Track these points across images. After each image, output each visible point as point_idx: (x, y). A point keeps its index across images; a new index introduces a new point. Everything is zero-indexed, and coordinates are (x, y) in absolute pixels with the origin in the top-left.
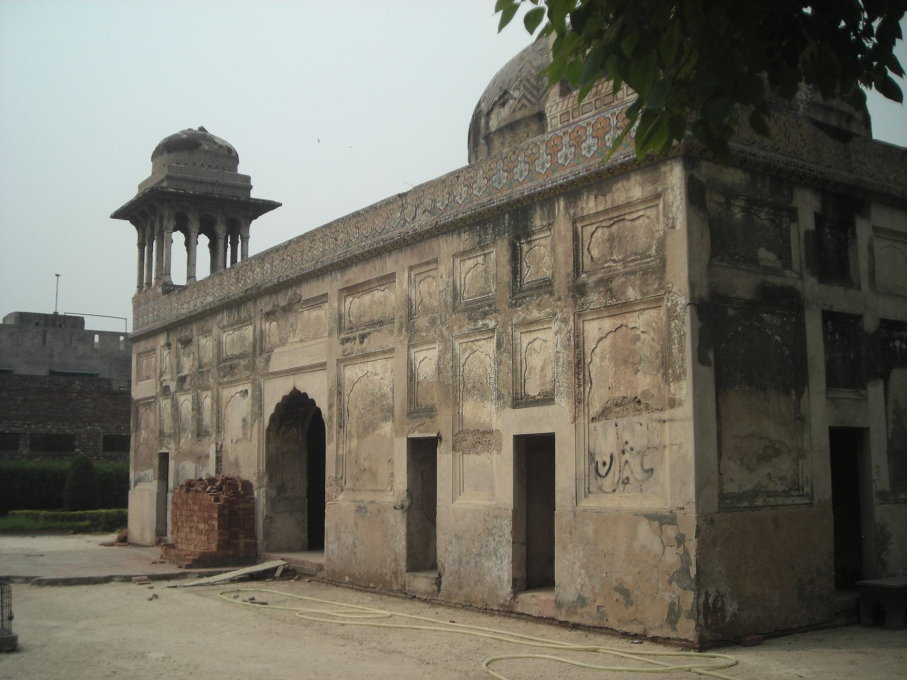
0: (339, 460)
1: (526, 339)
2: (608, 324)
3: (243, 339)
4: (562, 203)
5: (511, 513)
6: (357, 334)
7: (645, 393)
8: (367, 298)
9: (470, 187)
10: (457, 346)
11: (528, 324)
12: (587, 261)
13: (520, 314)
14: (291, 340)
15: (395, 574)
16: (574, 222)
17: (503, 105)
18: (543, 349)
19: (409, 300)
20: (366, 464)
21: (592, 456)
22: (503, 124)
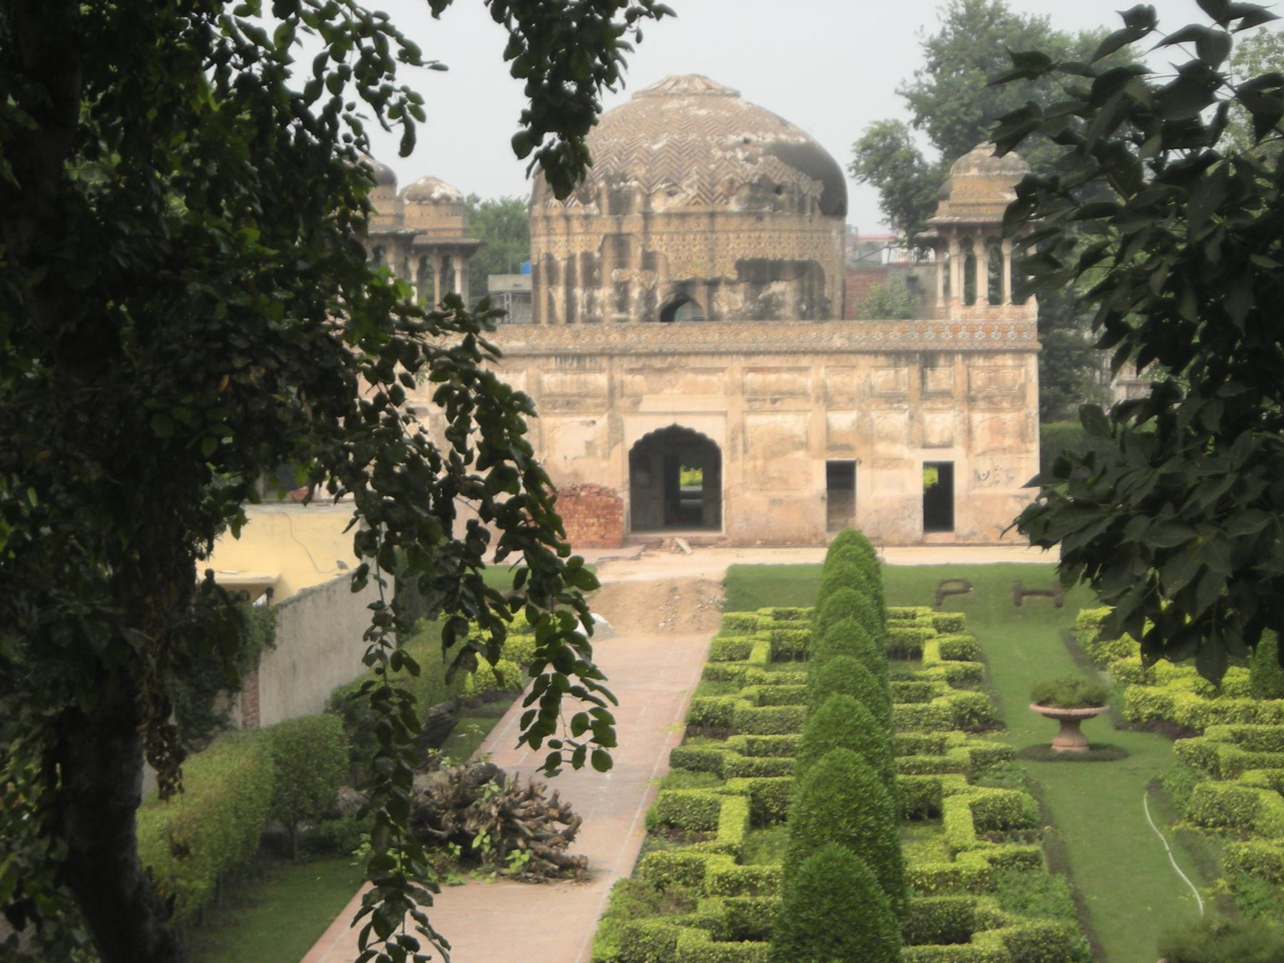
0: (745, 472)
1: (928, 417)
2: (987, 415)
3: (585, 383)
4: (960, 357)
5: (921, 498)
6: (768, 397)
7: (1010, 447)
8: (772, 377)
9: (886, 333)
10: (874, 415)
11: (932, 410)
12: (974, 386)
13: (928, 404)
14: (668, 391)
15: (815, 535)
16: (968, 367)
17: (671, 194)
18: (942, 422)
19: (824, 386)
20: (775, 475)
21: (976, 472)
22: (674, 211)
